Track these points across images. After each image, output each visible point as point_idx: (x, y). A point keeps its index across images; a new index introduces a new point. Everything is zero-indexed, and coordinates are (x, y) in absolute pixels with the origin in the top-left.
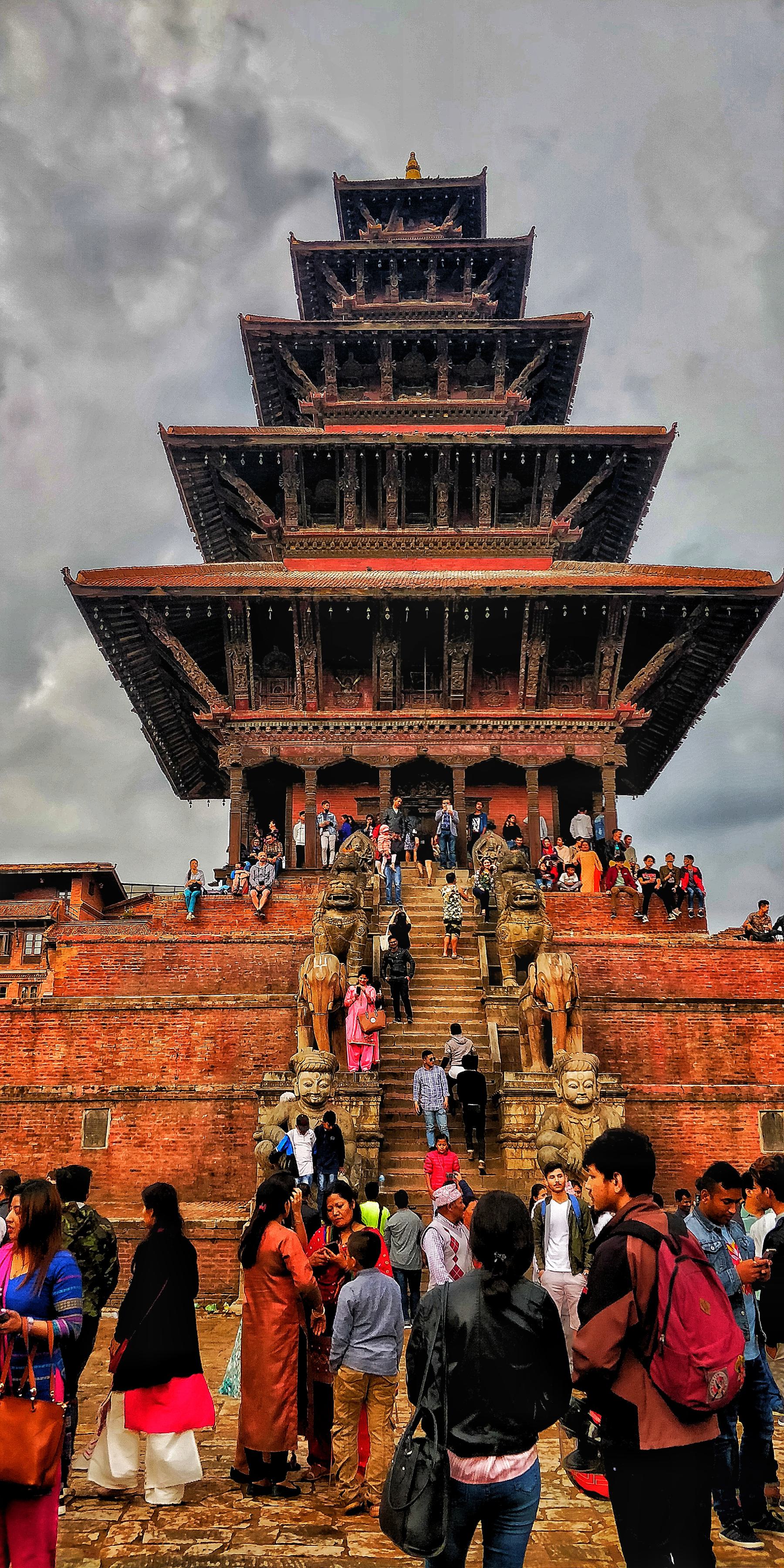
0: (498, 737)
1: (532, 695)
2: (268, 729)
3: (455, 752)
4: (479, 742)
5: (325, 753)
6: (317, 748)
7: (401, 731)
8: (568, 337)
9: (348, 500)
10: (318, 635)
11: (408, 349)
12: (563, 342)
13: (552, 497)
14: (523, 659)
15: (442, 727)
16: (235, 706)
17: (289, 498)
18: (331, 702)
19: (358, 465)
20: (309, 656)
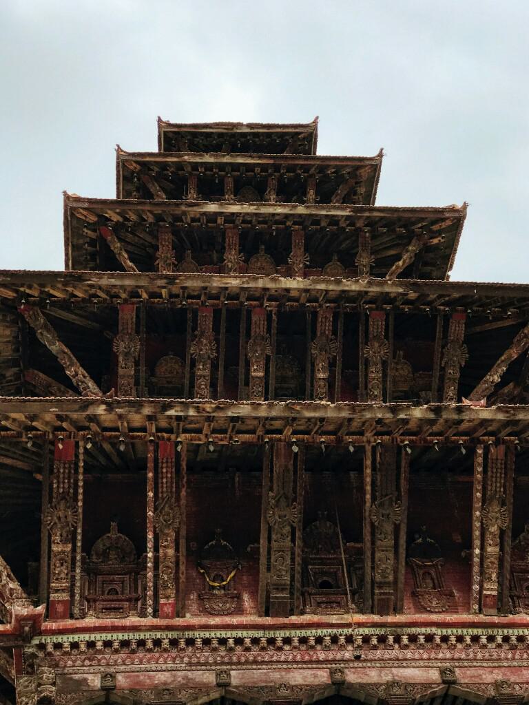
0: (448, 655)
1: (491, 589)
2: (99, 645)
3: (389, 678)
4: (422, 663)
5: (187, 685)
6: (174, 676)
7: (303, 648)
8: (439, 233)
9: (199, 373)
10: (183, 493)
11: (256, 250)
12: (435, 241)
13: (458, 375)
14: (477, 533)
15: (366, 639)
16: (49, 614)
17: (126, 370)
18: (194, 607)
19: (216, 328)
20: (168, 526)
